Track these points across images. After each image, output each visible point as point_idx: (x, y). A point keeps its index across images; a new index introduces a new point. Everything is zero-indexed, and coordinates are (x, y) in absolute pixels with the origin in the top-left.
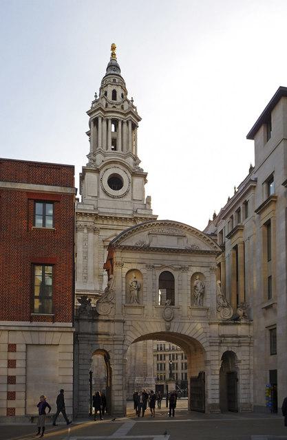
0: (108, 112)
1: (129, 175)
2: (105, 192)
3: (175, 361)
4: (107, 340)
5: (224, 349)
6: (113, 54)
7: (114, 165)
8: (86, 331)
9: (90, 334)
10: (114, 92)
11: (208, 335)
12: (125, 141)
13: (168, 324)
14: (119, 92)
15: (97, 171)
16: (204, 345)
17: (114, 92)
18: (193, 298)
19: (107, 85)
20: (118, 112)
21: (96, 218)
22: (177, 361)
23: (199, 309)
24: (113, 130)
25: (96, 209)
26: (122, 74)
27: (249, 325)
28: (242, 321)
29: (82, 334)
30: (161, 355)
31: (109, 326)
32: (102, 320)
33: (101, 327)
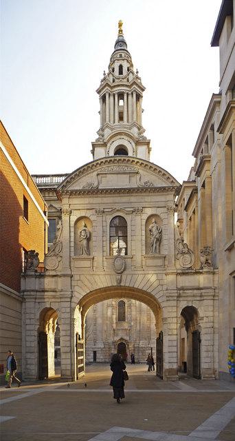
0: (115, 86)
4: (54, 297)
6: (121, 31)
8: (33, 288)
9: (37, 291)
10: (121, 67)
12: (130, 112)
14: (125, 65)
17: (121, 67)
18: (148, 246)
19: (114, 62)
20: (123, 85)
23: (154, 258)
26: (128, 49)
27: (214, 273)
29: (28, 291)
31: (56, 282)
32: (49, 276)
33: (48, 283)
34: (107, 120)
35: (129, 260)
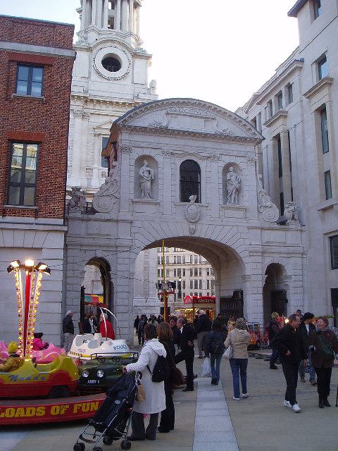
1: (129, 55)
2: (98, 73)
3: (198, 278)
5: (268, 261)
7: (110, 44)
11: (247, 242)
13: (193, 226)
15: (89, 49)
16: (241, 255)
21: (86, 101)
22: (200, 278)
24: (110, 7)
25: (86, 92)
28: (290, 227)
30: (179, 270)
34: (93, 22)
35: (204, 210)
